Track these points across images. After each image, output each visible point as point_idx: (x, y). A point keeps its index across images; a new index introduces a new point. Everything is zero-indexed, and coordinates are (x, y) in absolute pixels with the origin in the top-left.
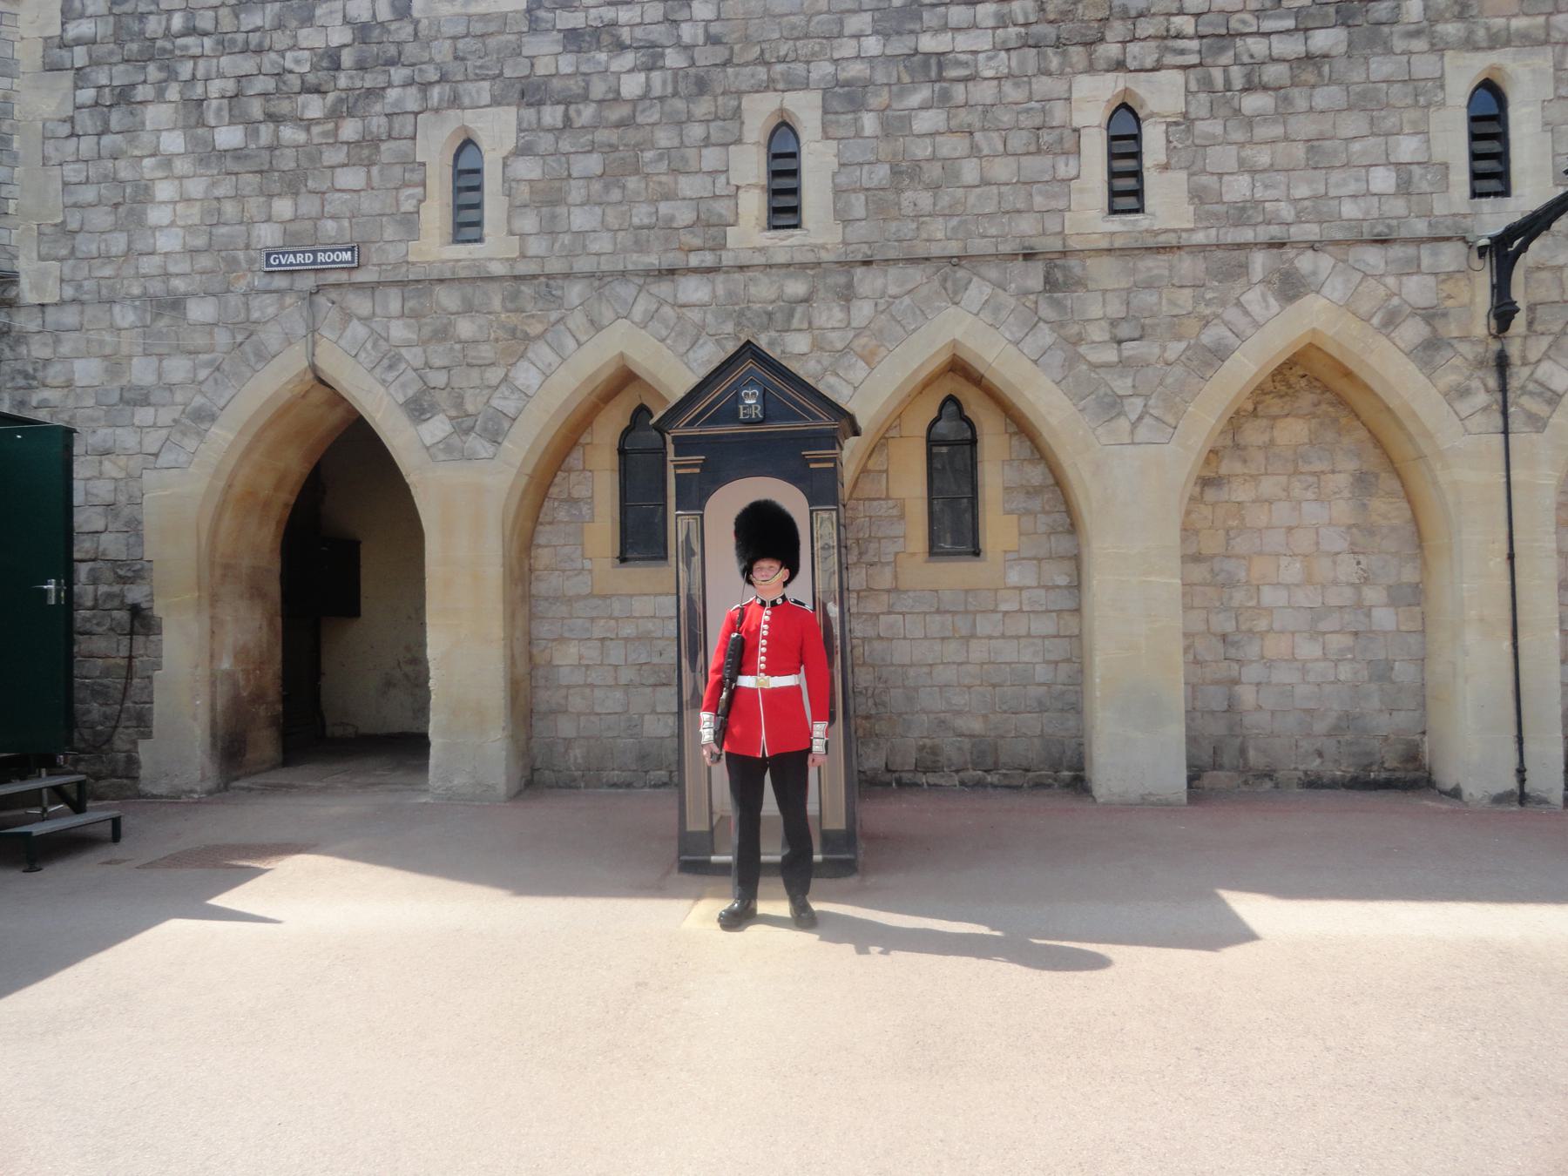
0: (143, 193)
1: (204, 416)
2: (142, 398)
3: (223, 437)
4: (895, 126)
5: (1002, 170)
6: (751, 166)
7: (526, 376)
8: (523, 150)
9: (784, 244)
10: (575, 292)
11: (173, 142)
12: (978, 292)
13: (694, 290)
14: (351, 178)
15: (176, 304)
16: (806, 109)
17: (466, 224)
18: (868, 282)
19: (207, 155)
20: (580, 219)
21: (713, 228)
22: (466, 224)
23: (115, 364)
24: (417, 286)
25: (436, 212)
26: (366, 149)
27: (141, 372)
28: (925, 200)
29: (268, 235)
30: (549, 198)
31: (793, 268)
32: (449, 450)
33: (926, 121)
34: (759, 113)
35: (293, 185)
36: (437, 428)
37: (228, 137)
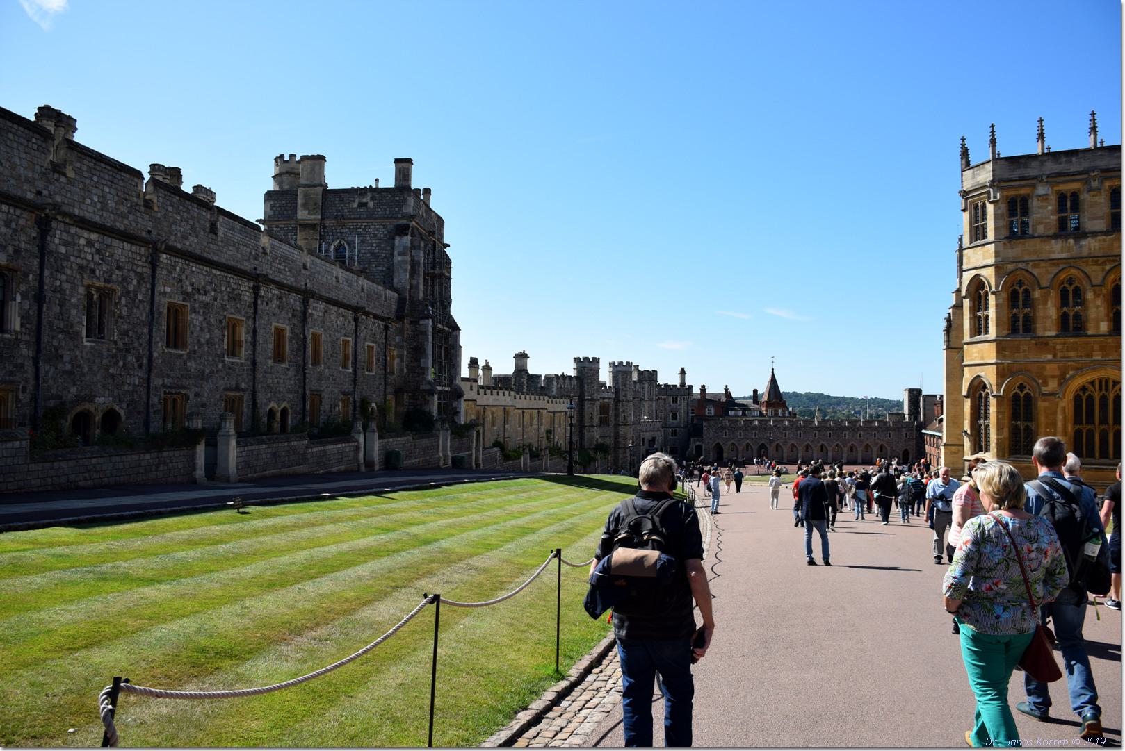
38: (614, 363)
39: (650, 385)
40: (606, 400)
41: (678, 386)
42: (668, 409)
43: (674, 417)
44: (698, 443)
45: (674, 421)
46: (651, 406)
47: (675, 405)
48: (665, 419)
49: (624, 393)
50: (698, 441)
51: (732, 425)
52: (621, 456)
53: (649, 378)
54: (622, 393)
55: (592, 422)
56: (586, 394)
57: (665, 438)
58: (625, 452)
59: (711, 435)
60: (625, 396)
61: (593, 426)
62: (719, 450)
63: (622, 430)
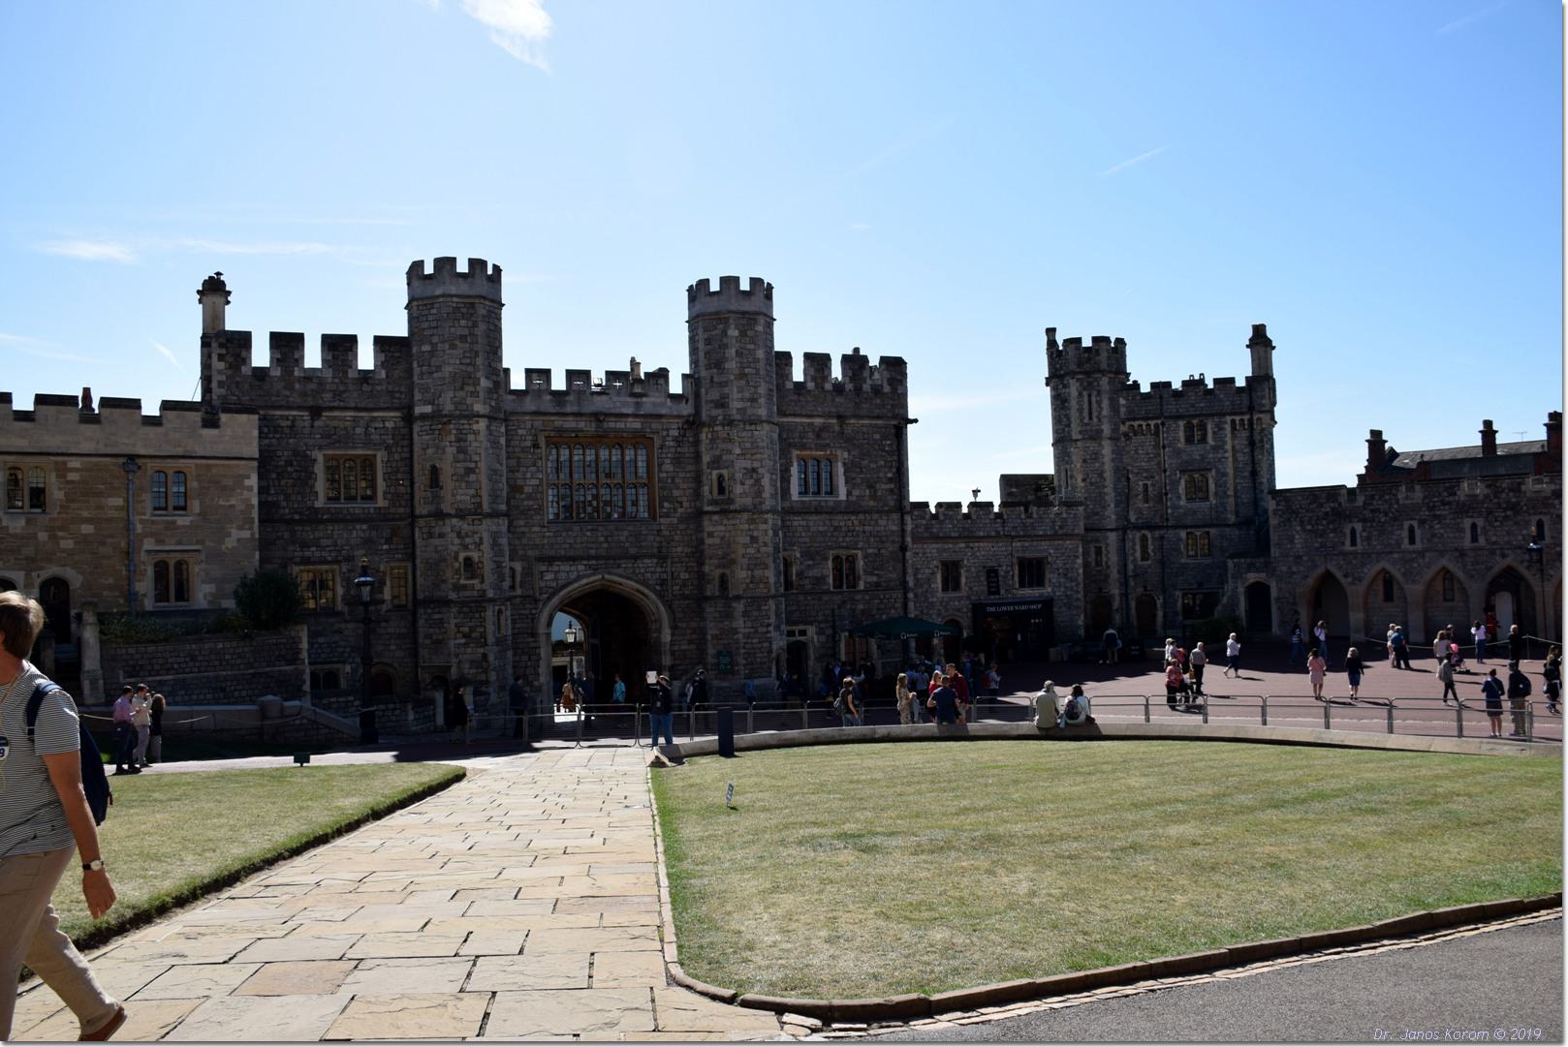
0: (1293, 537)
1: (1306, 577)
2: (1294, 573)
3: (1310, 581)
4: (1431, 527)
5: (1451, 535)
6: (1405, 534)
7: (1366, 570)
8: (1364, 531)
9: (1411, 548)
10: (1374, 556)
11: (1298, 528)
12: (1447, 557)
13: (1396, 556)
14: (1332, 535)
15: (1300, 557)
16: (1415, 524)
17: (1353, 543)
18: (1427, 554)
19: (1304, 530)
20: (1375, 543)
21: (1399, 544)
22: (1353, 543)
23: (1290, 568)
24: (1344, 554)
25: (1348, 542)
26: (1334, 531)
27: (1294, 569)
28: (1437, 540)
29: (1317, 545)
30: (1368, 539)
31: (1414, 552)
32: (1352, 583)
33: (1437, 526)
34: (1406, 525)
35: (1321, 536)
36: (1350, 579)
37: (1309, 527)
38: (1108, 355)
39: (1088, 386)
40: (636, 424)
41: (1240, 383)
42: (1170, 463)
43: (1197, 491)
44: (1252, 577)
45: (1196, 505)
46: (1096, 456)
47: (1196, 452)
48: (1161, 497)
49: (714, 395)
50: (1250, 568)
51: (1377, 503)
52: (712, 630)
53: (1079, 365)
54: (710, 395)
55: (437, 498)
56: (417, 396)
57: (1162, 563)
58: (728, 615)
59: (1298, 539)
60: (722, 403)
61: (440, 515)
62: (1326, 593)
63: (715, 529)
